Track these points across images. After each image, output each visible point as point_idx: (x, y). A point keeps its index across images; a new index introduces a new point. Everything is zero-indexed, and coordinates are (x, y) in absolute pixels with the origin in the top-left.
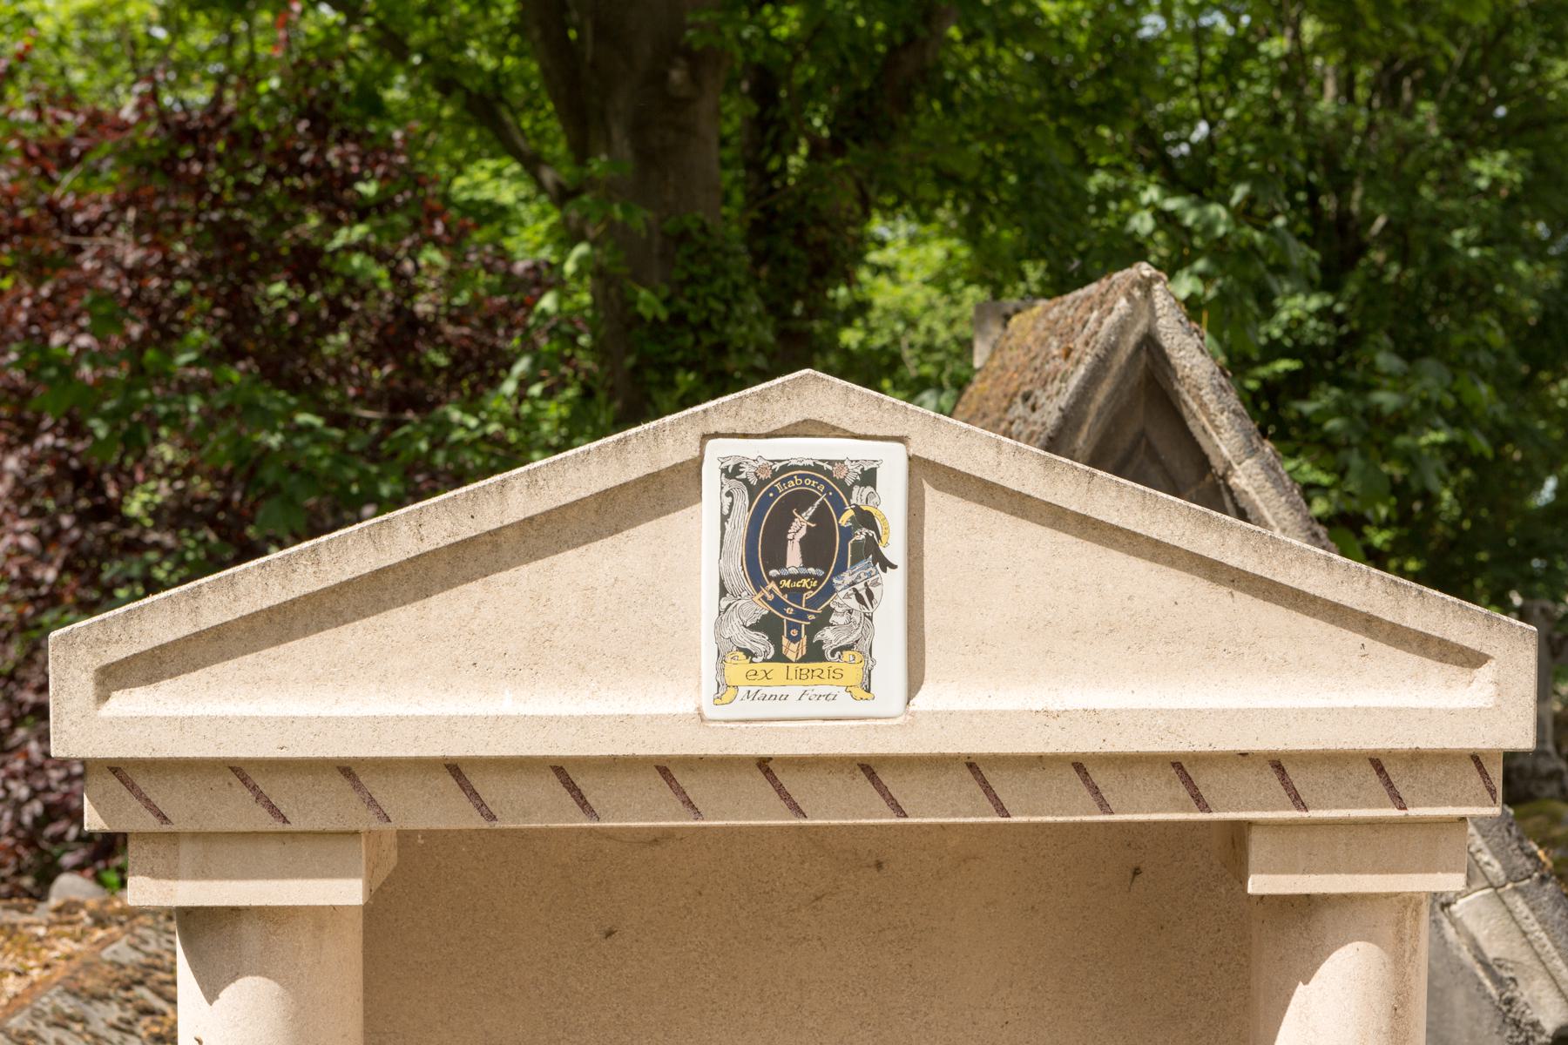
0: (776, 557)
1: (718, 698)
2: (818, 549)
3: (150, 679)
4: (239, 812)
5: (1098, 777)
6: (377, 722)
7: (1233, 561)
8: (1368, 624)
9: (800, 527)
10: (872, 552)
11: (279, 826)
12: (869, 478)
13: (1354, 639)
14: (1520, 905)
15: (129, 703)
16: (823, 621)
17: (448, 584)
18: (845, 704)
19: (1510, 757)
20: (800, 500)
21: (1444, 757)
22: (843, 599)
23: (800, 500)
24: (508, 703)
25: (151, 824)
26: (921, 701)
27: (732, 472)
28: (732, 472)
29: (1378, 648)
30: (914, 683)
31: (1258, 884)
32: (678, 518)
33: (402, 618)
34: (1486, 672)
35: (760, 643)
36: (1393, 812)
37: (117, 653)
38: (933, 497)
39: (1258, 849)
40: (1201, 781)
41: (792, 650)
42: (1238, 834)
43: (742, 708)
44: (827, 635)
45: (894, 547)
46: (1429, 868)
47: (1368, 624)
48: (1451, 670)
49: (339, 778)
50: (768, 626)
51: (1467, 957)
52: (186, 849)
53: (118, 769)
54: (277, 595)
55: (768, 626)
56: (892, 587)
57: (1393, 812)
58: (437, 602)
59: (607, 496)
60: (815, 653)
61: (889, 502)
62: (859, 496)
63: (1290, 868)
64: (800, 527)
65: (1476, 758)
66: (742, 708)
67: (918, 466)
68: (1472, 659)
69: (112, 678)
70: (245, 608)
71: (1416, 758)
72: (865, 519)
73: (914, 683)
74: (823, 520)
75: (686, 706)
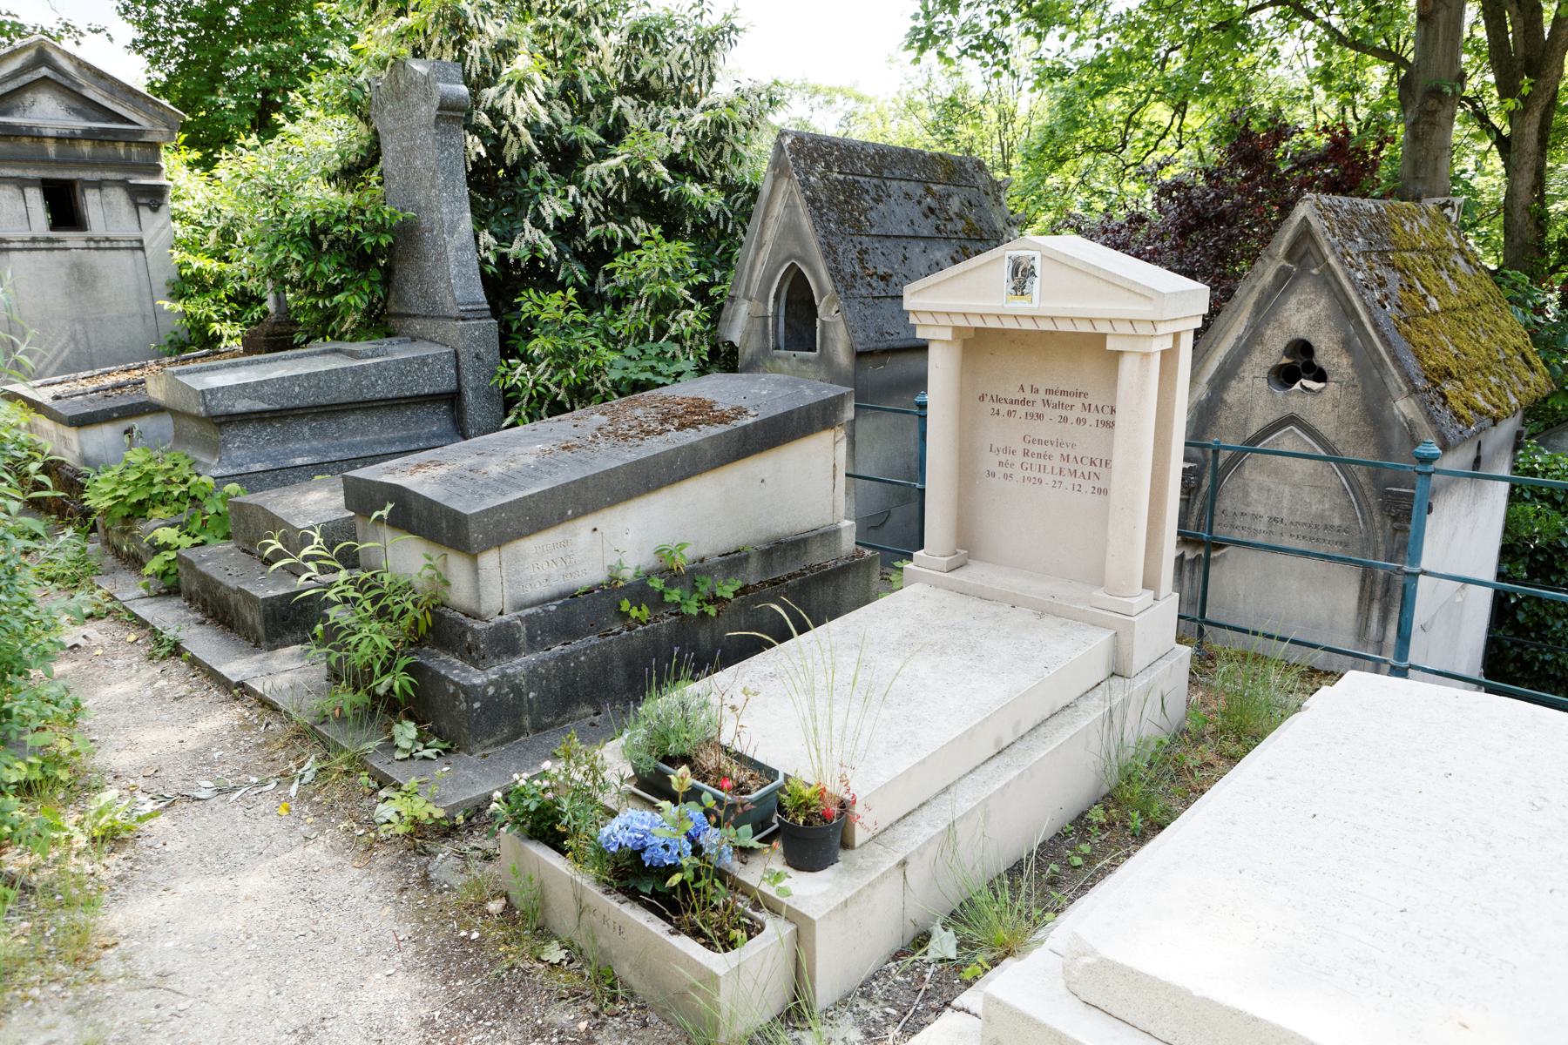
10: (1033, 274)
22: (1028, 284)
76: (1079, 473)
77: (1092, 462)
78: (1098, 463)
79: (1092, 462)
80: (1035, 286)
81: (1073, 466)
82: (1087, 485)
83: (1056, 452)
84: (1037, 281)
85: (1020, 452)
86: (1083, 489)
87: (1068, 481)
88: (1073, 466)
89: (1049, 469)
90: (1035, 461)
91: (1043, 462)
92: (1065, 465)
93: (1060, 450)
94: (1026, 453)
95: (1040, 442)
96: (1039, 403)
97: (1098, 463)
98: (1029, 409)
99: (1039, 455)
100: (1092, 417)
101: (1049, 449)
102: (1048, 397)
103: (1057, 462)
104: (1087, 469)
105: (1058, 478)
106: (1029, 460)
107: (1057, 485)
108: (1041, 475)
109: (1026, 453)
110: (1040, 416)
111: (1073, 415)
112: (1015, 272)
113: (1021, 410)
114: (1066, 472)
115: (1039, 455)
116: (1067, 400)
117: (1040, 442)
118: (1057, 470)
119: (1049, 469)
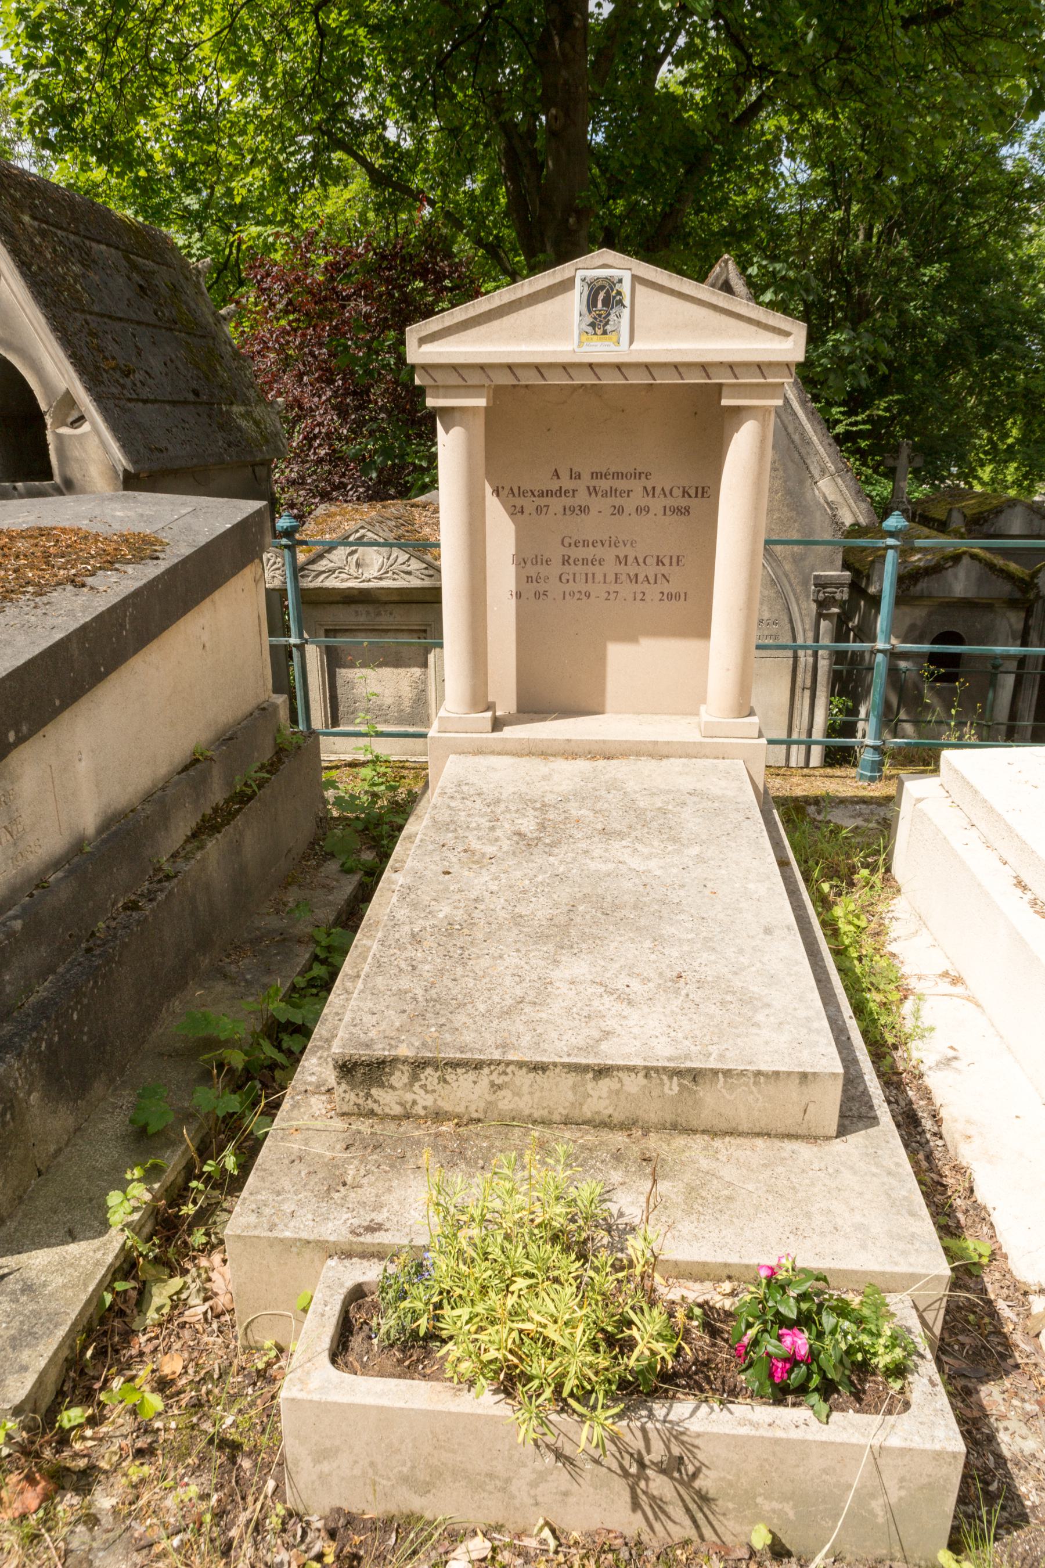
0: (595, 305)
1: (579, 346)
2: (606, 302)
3: (432, 341)
4: (453, 379)
5: (681, 370)
6: (490, 353)
7: (721, 304)
8: (758, 324)
9: (602, 295)
10: (620, 303)
11: (463, 383)
12: (620, 281)
13: (754, 328)
14: (839, 481)
15: (427, 348)
16: (607, 323)
17: (508, 314)
18: (613, 347)
19: (799, 365)
20: (602, 288)
21: (778, 364)
22: (612, 317)
23: (602, 288)
24: (523, 348)
25: (432, 383)
26: (633, 347)
27: (583, 280)
28: (583, 280)
29: (761, 331)
30: (631, 341)
31: (724, 402)
32: (568, 294)
33: (496, 324)
34: (791, 338)
35: (590, 329)
36: (762, 380)
37: (423, 334)
38: (638, 287)
39: (725, 391)
40: (709, 371)
41: (599, 332)
42: (721, 385)
43: (585, 349)
44: (609, 328)
45: (627, 302)
46: (773, 398)
47: (758, 324)
48: (782, 338)
49: (480, 371)
50: (592, 325)
51: (822, 501)
52: (441, 391)
53: (425, 367)
54: (464, 317)
55: (592, 325)
56: (626, 313)
57: (762, 380)
58: (505, 319)
59: (550, 288)
60: (605, 333)
61: (626, 288)
62: (618, 286)
63: (733, 397)
64: (602, 295)
65: (788, 365)
66: (585, 349)
67: (635, 278)
68: (787, 334)
69: (422, 341)
70: (456, 321)
71: (770, 364)
72: (619, 293)
73: (631, 341)
74: (608, 293)
75: (570, 348)
76: (641, 578)
77: (659, 561)
78: (666, 561)
79: (659, 561)
80: (622, 320)
81: (632, 570)
82: (653, 591)
83: (609, 554)
84: (626, 313)
85: (557, 560)
86: (647, 597)
87: (627, 589)
88: (632, 570)
89: (599, 577)
90: (579, 569)
91: (590, 569)
92: (621, 569)
93: (615, 551)
94: (566, 561)
95: (585, 544)
96: (583, 492)
97: (666, 561)
98: (568, 501)
99: (585, 562)
100: (657, 504)
101: (598, 552)
102: (594, 483)
103: (610, 567)
104: (651, 570)
105: (614, 587)
106: (571, 569)
107: (612, 596)
108: (589, 587)
109: (566, 561)
110: (584, 510)
111: (630, 504)
112: (592, 303)
113: (556, 504)
114: (623, 578)
115: (585, 562)
116: (621, 484)
117: (585, 544)
118: (611, 578)
119: (599, 577)
